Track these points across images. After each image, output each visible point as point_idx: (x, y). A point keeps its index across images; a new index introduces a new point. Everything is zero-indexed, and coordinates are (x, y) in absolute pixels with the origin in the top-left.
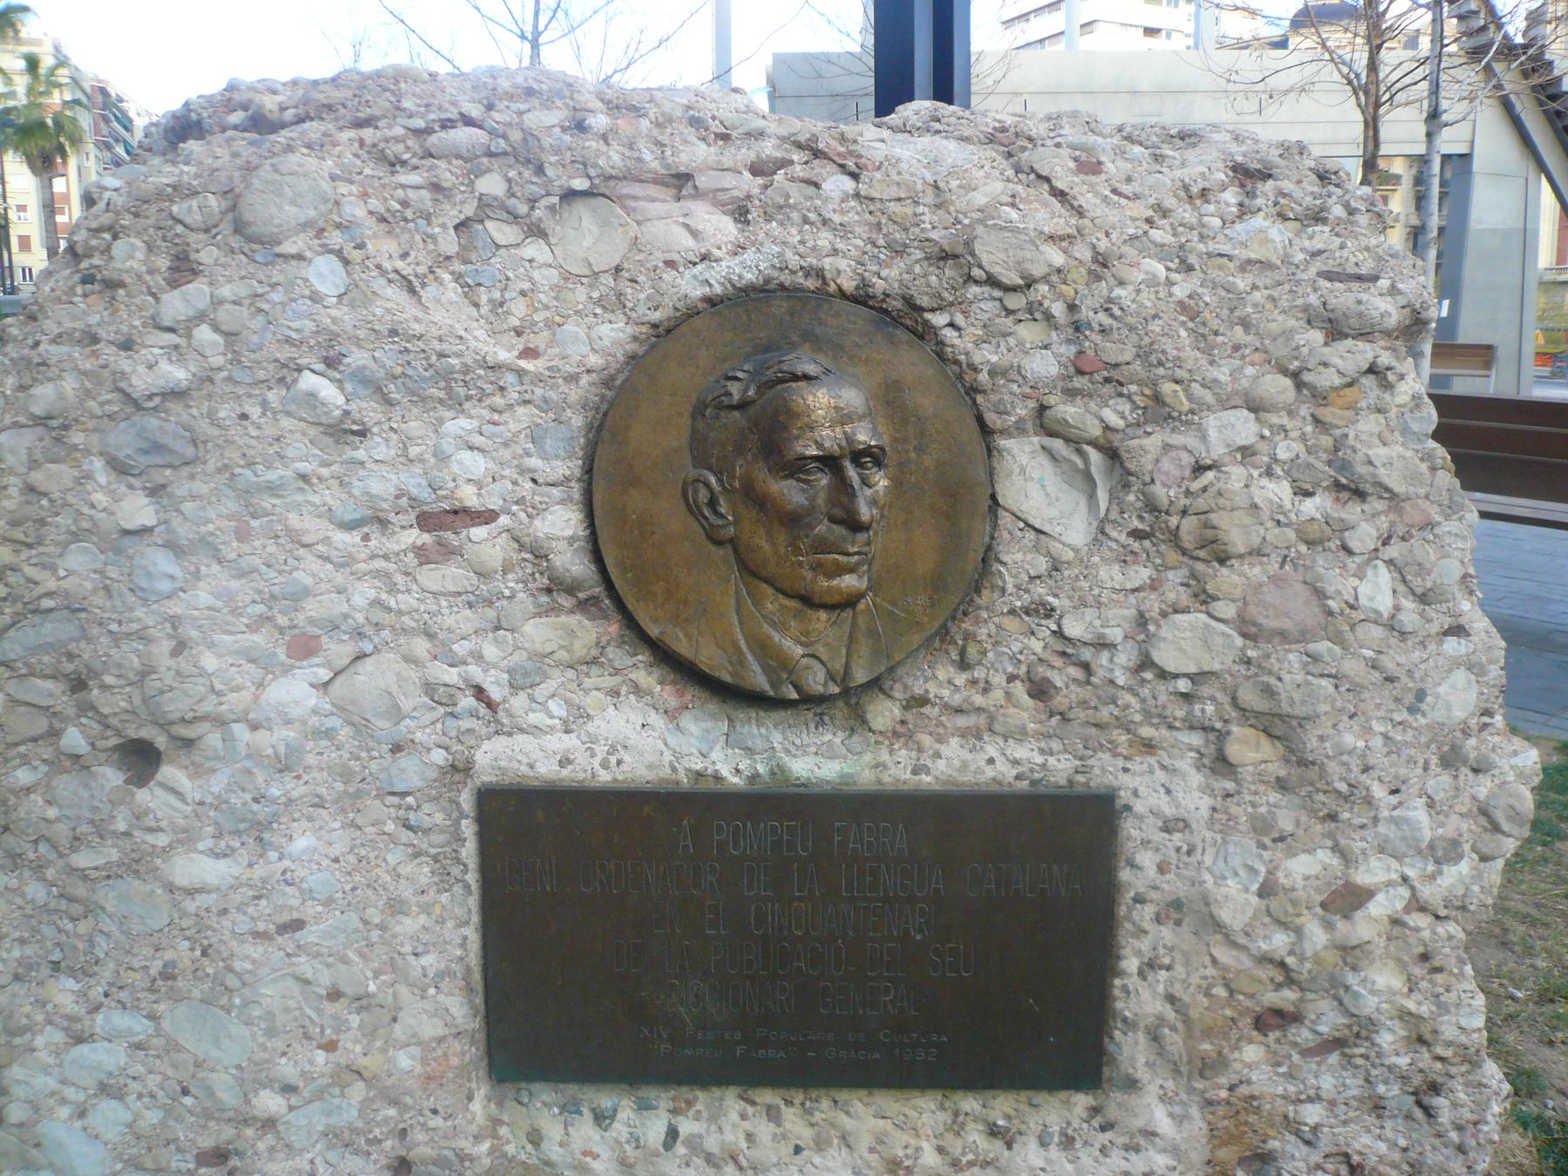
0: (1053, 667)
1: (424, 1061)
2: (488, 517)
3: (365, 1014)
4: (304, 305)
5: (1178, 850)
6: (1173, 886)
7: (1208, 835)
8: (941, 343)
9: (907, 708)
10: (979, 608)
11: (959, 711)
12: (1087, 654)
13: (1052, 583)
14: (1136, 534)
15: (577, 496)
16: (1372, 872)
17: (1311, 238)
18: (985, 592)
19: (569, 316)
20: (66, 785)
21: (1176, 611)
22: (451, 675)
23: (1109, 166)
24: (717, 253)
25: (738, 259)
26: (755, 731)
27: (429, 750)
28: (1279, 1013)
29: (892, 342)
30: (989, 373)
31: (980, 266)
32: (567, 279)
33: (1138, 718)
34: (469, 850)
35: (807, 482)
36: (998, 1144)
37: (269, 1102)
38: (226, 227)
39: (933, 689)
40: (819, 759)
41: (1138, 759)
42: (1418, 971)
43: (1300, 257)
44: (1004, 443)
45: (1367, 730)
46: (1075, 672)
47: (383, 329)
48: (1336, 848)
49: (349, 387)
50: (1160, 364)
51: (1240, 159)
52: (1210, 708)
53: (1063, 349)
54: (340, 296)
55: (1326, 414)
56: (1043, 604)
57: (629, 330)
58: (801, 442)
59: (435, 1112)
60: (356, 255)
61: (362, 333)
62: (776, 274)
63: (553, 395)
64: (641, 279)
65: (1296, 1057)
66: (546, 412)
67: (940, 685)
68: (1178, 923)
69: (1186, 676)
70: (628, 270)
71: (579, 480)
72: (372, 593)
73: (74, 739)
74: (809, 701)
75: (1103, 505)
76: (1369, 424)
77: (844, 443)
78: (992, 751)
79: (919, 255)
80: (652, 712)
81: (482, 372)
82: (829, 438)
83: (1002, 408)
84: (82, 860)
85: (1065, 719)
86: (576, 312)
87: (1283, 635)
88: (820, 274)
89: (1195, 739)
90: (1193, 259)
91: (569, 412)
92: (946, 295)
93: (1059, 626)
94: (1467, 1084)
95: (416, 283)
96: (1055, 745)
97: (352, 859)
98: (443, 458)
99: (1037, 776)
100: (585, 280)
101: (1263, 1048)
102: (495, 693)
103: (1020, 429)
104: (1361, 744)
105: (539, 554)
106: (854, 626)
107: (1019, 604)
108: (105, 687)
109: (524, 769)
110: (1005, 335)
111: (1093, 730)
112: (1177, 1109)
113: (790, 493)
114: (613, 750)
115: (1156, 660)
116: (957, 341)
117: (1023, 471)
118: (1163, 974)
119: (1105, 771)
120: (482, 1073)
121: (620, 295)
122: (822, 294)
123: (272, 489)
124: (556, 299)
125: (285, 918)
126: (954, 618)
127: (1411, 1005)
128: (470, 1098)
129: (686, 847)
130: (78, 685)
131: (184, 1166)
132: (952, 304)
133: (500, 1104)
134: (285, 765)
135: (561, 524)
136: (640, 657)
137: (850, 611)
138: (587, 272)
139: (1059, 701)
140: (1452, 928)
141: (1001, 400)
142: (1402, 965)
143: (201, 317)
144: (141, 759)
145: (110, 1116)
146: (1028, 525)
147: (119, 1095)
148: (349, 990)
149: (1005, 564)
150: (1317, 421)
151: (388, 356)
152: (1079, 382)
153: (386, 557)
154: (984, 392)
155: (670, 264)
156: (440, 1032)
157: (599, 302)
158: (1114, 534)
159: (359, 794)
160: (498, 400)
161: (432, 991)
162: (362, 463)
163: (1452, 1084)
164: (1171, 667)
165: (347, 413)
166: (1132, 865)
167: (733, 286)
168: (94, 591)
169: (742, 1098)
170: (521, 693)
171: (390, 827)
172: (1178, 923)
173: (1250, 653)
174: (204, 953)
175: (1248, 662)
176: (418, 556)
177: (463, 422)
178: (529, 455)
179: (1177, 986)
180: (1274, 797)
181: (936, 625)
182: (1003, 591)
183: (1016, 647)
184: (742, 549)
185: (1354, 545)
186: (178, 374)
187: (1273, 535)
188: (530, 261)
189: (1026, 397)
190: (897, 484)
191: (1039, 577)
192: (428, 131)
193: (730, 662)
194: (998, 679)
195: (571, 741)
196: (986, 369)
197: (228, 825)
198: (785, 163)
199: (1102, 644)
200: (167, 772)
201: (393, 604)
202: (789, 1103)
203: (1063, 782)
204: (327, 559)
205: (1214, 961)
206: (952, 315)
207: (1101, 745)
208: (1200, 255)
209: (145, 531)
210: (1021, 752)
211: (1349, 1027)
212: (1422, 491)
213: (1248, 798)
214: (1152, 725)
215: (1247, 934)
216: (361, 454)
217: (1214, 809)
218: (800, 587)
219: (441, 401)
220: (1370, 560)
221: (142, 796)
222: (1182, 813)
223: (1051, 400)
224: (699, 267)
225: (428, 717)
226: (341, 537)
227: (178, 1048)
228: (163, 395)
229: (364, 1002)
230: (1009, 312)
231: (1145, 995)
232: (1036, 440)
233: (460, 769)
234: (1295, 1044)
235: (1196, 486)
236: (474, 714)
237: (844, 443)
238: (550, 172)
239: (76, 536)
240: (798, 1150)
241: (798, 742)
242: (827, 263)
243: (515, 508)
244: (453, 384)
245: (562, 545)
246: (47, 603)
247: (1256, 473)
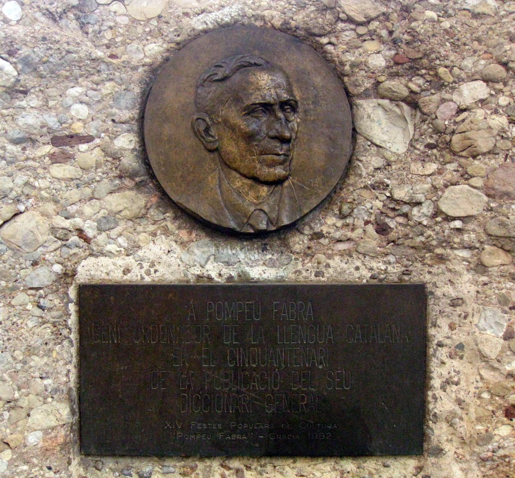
0: (389, 217)
2: (88, 139)
3: (12, 412)
5: (460, 316)
6: (460, 337)
7: (476, 306)
8: (325, 52)
9: (311, 239)
10: (349, 185)
11: (339, 241)
12: (405, 209)
13: (386, 172)
14: (430, 146)
15: (136, 128)
17: (509, 6)
18: (352, 177)
19: (134, 40)
21: (452, 184)
22: (67, 224)
24: (209, 8)
25: (220, 11)
26: (230, 252)
27: (52, 265)
29: (298, 48)
30: (350, 66)
31: (344, 12)
32: (133, 22)
33: (434, 243)
34: (73, 320)
35: (257, 117)
39: (325, 229)
40: (264, 268)
41: (436, 267)
43: (503, 13)
44: (359, 102)
46: (401, 220)
47: (40, 36)
49: (20, 66)
50: (437, 58)
52: (473, 236)
53: (388, 53)
54: (18, 22)
56: (383, 183)
58: (253, 97)
59: (50, 468)
61: (28, 39)
62: (240, 18)
63: (124, 76)
64: (171, 21)
66: (120, 85)
67: (329, 226)
68: (461, 358)
70: (165, 17)
71: (137, 120)
72: (25, 178)
75: (412, 132)
77: (275, 98)
78: (358, 263)
79: (313, 8)
80: (174, 244)
81: (89, 62)
83: (357, 83)
86: (137, 38)
88: (263, 18)
89: (465, 254)
90: (451, 11)
91: (132, 86)
92: (327, 28)
93: (391, 194)
95: (56, 16)
96: (391, 258)
97: (8, 323)
99: (382, 276)
100: (142, 23)
101: (509, 428)
102: (90, 233)
103: (366, 95)
105: (115, 157)
106: (281, 195)
107: (369, 182)
109: (104, 276)
110: (357, 48)
111: (411, 251)
112: (465, 466)
114: (153, 265)
115: (444, 210)
116: (333, 51)
117: (369, 116)
118: (454, 388)
119: (420, 274)
120: (76, 448)
121: (160, 30)
122: (263, 29)
124: (127, 31)
126: (335, 192)
128: (69, 463)
129: (192, 317)
132: (330, 32)
133: (86, 469)
136: (168, 214)
137: (279, 187)
138: (145, 19)
139: (393, 235)
141: (356, 80)
146: (372, 143)
149: (361, 161)
151: (40, 51)
153: (34, 159)
154: (347, 75)
155: (186, 14)
156: (54, 423)
158: (418, 146)
159: (15, 289)
160: (96, 78)
161: (50, 400)
162: (24, 108)
164: (451, 213)
166: (435, 325)
167: (218, 24)
169: (222, 466)
170: (103, 233)
171: (29, 307)
172: (461, 358)
173: (492, 205)
175: (491, 210)
176: (51, 159)
178: (112, 107)
179: (462, 393)
181: (326, 194)
183: (368, 205)
184: (223, 154)
187: (501, 144)
188: (115, 12)
189: (371, 77)
191: (379, 169)
193: (216, 214)
194: (360, 223)
195: (130, 260)
196: (348, 64)
201: (36, 184)
202: (248, 468)
203: (396, 279)
205: (482, 378)
206: (330, 38)
207: (416, 259)
208: (454, 9)
210: (374, 264)
213: (495, 285)
214: (443, 247)
215: (499, 361)
216: (24, 103)
217: (478, 292)
219: (67, 78)
222: (460, 295)
223: (382, 79)
224: (201, 16)
226: (10, 147)
229: (12, 404)
231: (445, 400)
232: (375, 100)
233: (68, 275)
237: (275, 98)
241: (253, 258)
242: (266, 13)
243: (103, 135)
245: (127, 153)
247: (489, 112)
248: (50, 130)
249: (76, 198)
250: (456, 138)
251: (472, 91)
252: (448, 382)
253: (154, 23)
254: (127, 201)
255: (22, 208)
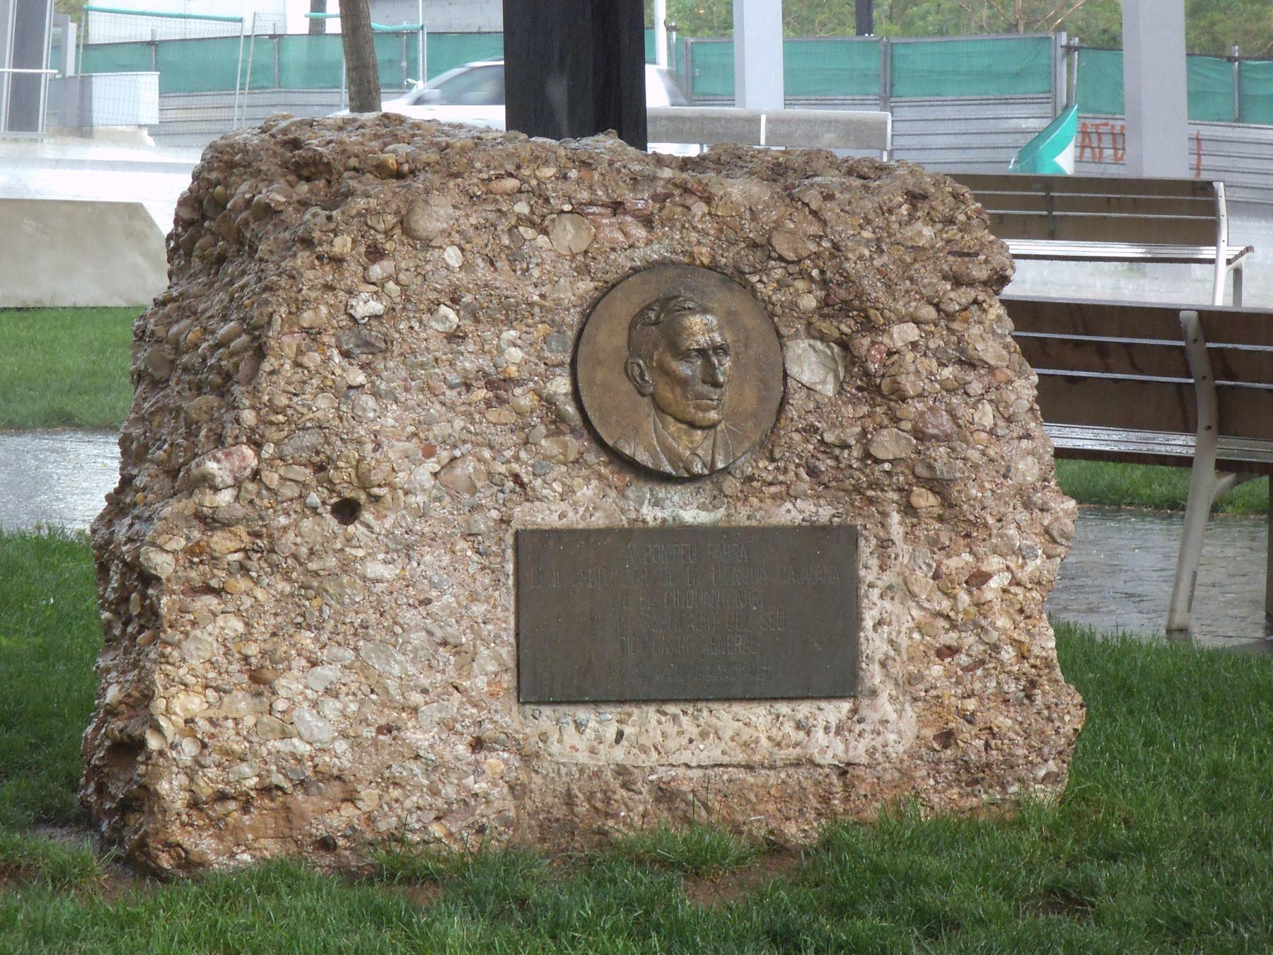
1: (489, 684)
4: (444, 272)
11: (771, 484)
14: (859, 389)
20: (307, 524)
22: (502, 469)
23: (838, 195)
28: (949, 648)
34: (510, 567)
36: (801, 735)
37: (416, 698)
38: (398, 231)
42: (1019, 618)
43: (940, 244)
45: (982, 488)
46: (830, 462)
48: (971, 552)
51: (910, 188)
52: (902, 478)
55: (956, 326)
56: (812, 426)
57: (592, 285)
60: (468, 246)
65: (960, 673)
69: (888, 461)
72: (462, 424)
73: (314, 498)
74: (694, 478)
75: (842, 375)
76: (976, 330)
79: (743, 245)
82: (703, 340)
84: (313, 566)
85: (827, 487)
87: (936, 437)
88: (691, 255)
94: (1049, 680)
98: (501, 352)
104: (980, 495)
108: (337, 468)
110: (788, 286)
113: (684, 369)
121: (587, 266)
123: (422, 366)
125: (422, 597)
127: (1015, 636)
130: (320, 468)
131: (369, 735)
134: (422, 514)
135: (560, 385)
140: (1034, 594)
142: (1010, 617)
143: (389, 278)
144: (347, 511)
145: (331, 707)
147: (337, 696)
148: (451, 640)
150: (948, 329)
152: (826, 311)
153: (470, 404)
157: (576, 269)
160: (530, 321)
163: (1041, 680)
164: (880, 456)
165: (459, 326)
168: (333, 418)
169: (658, 711)
171: (469, 553)
172: (892, 599)
174: (381, 615)
175: (919, 453)
177: (512, 332)
180: (937, 526)
182: (792, 419)
185: (971, 391)
186: (377, 307)
190: (736, 363)
192: (490, 180)
194: (792, 467)
195: (564, 506)
197: (392, 546)
198: (669, 195)
199: (845, 446)
200: (367, 516)
204: (443, 404)
209: (362, 386)
211: (985, 651)
212: (1004, 364)
216: (462, 348)
218: (688, 418)
220: (979, 401)
221: (351, 528)
225: (488, 493)
227: (368, 667)
228: (370, 317)
230: (791, 274)
231: (878, 642)
234: (958, 665)
235: (888, 363)
236: (513, 491)
238: (552, 201)
239: (322, 390)
240: (691, 741)
242: (696, 249)
244: (511, 313)
245: (562, 398)
246: (309, 424)
248: (486, 375)
249: (510, 443)
250: (886, 382)
251: (904, 333)
252: (880, 623)
253: (580, 258)
255: (457, 453)
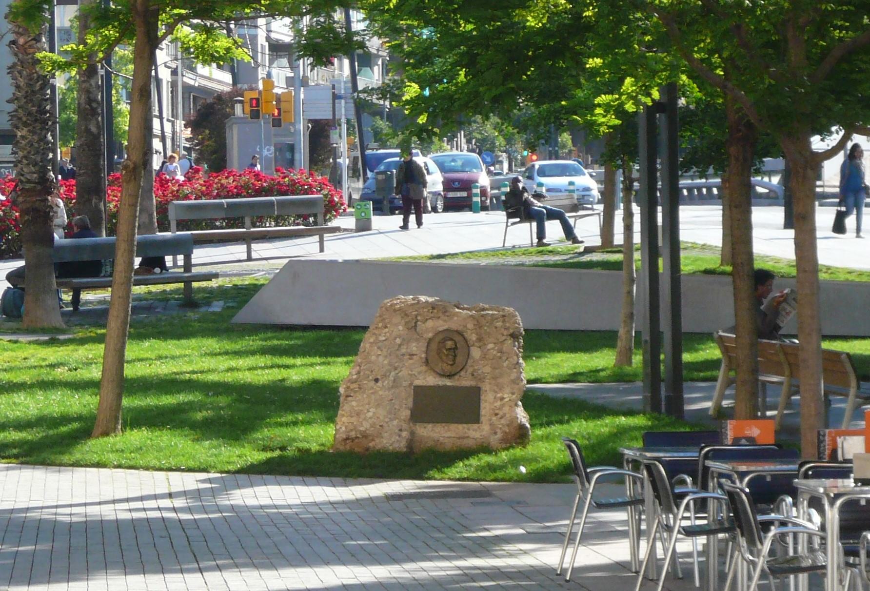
16: (506, 396)
119: (480, 385)
144: (377, 380)
233: (411, 384)
251: (491, 346)
254: (424, 368)
